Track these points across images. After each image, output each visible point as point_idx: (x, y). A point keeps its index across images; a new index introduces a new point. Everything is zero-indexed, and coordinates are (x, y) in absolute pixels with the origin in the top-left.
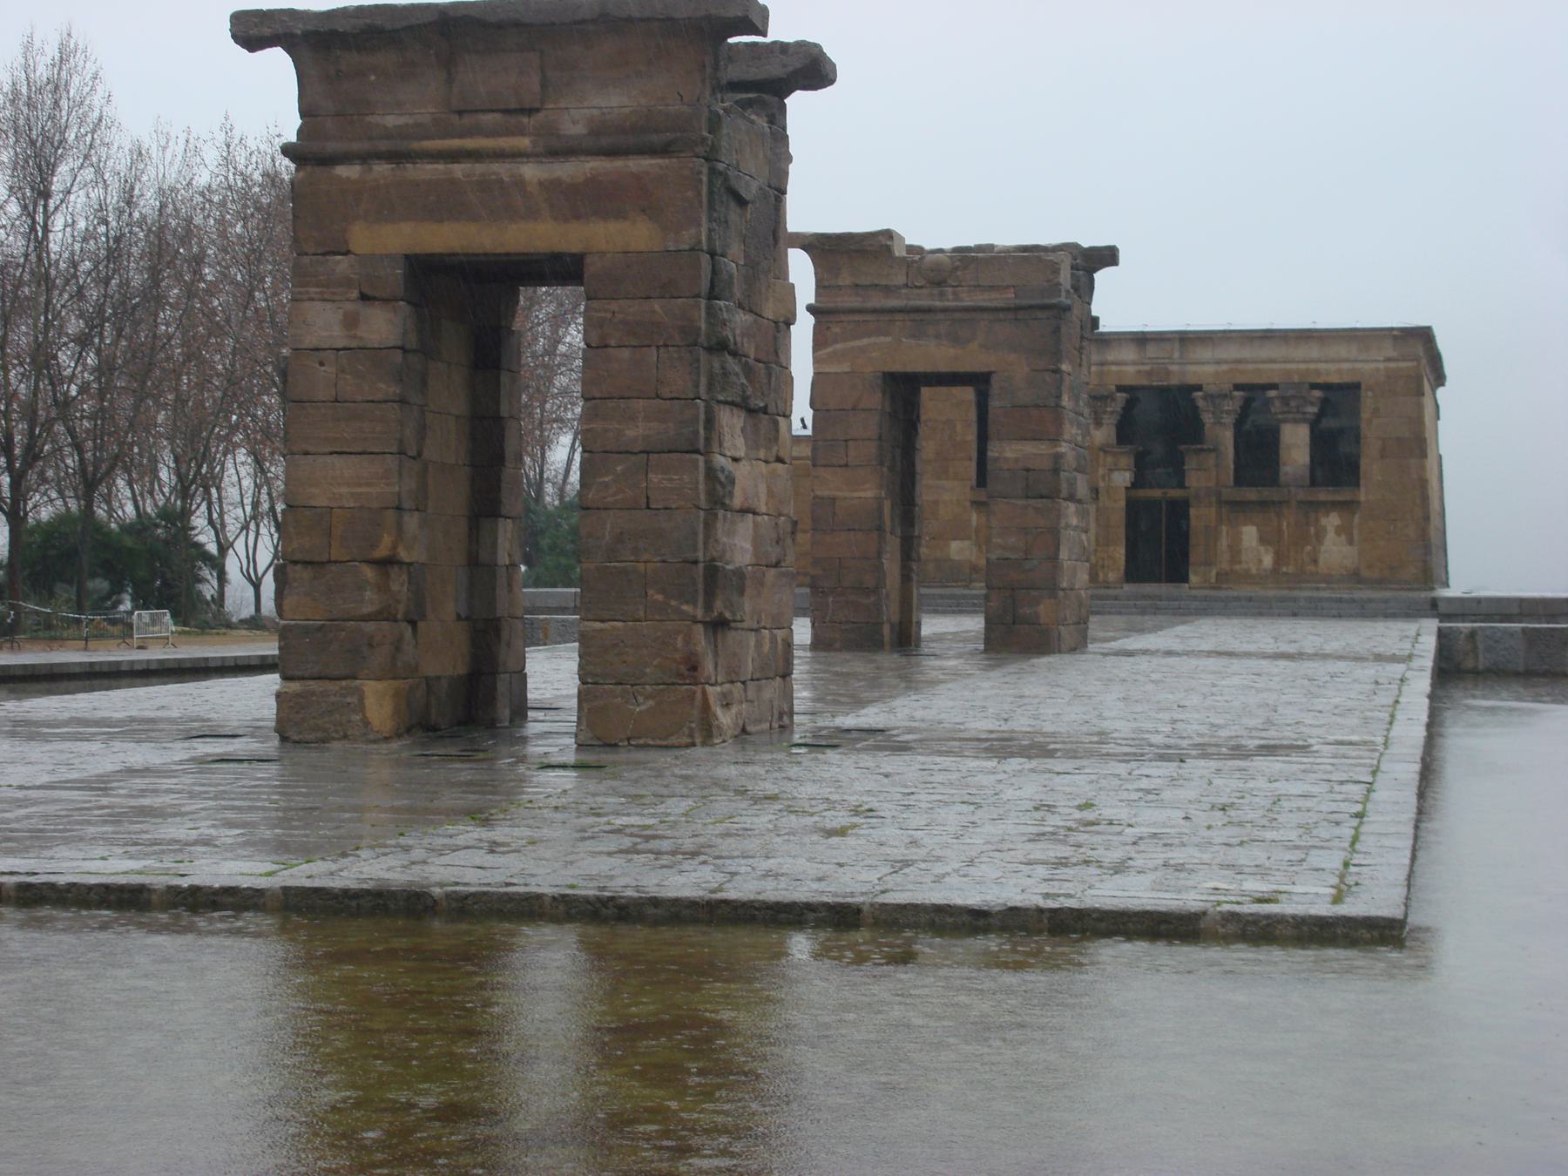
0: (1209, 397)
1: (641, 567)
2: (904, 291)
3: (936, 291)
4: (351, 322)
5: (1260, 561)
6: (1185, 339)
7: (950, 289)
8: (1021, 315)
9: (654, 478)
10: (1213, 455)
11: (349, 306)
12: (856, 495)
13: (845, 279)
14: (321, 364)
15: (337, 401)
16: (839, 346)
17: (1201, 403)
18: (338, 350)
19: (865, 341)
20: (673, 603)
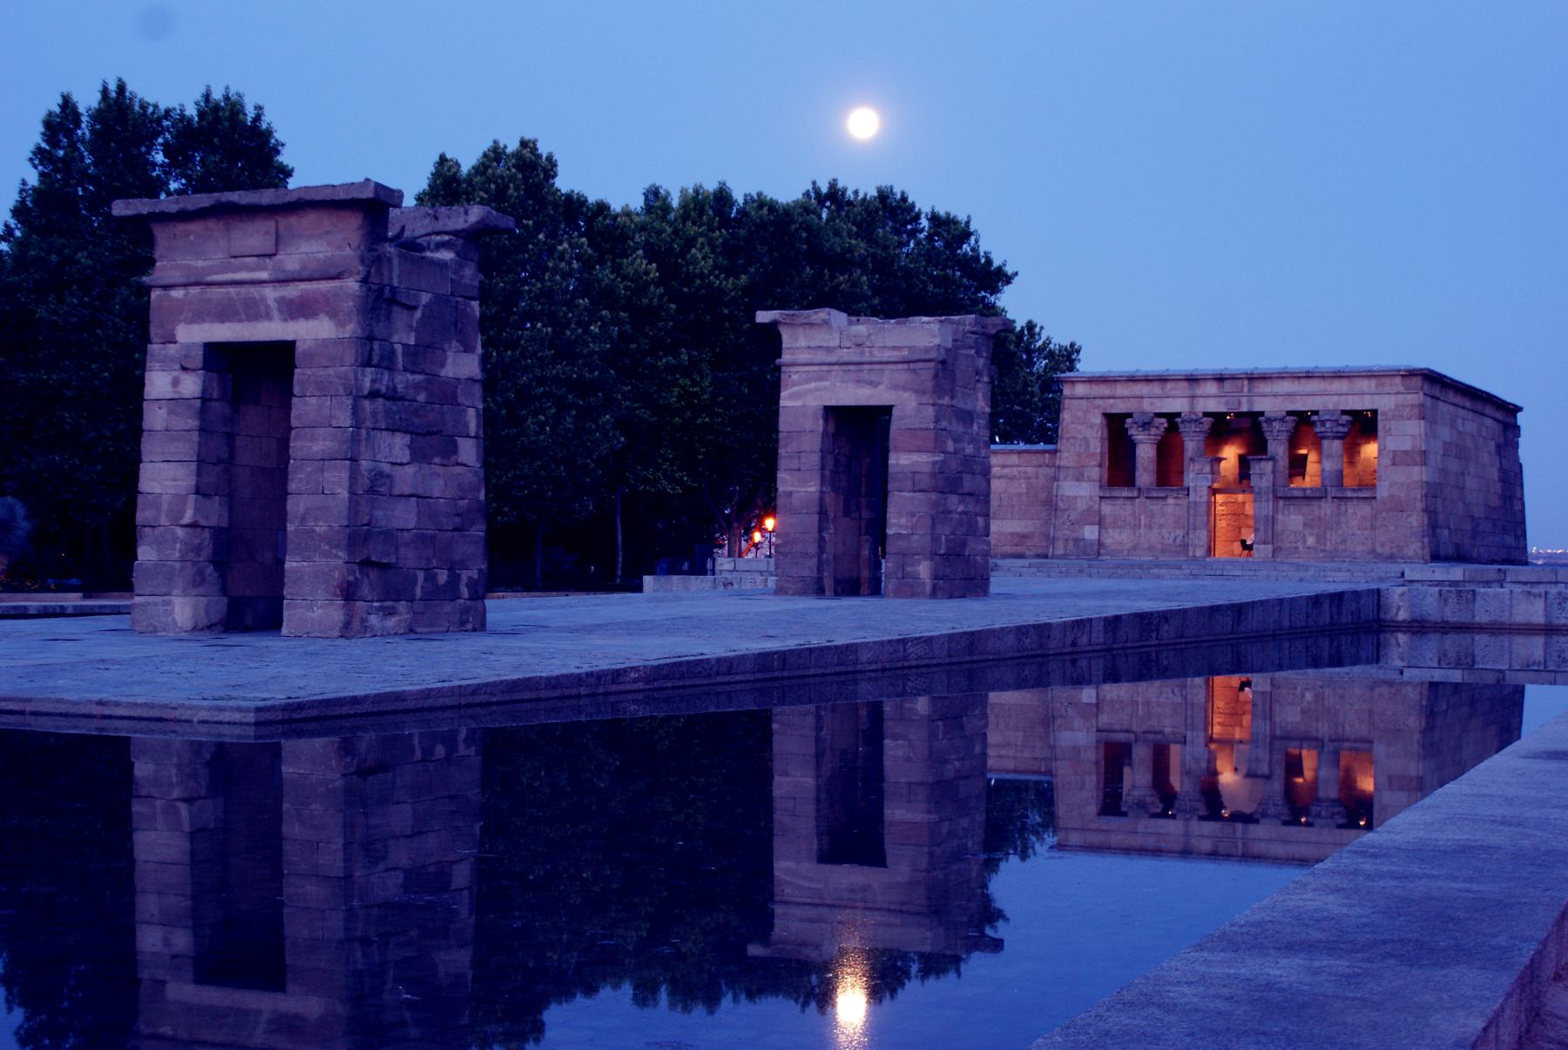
0: (1269, 421)
1: (317, 529)
2: (839, 350)
3: (859, 350)
4: (176, 383)
5: (1305, 542)
6: (1252, 378)
7: (867, 350)
8: (912, 366)
9: (326, 474)
10: (1271, 463)
11: (175, 374)
12: (804, 490)
13: (802, 342)
14: (160, 408)
16: (796, 389)
17: (1264, 425)
19: (813, 385)
20: (334, 551)
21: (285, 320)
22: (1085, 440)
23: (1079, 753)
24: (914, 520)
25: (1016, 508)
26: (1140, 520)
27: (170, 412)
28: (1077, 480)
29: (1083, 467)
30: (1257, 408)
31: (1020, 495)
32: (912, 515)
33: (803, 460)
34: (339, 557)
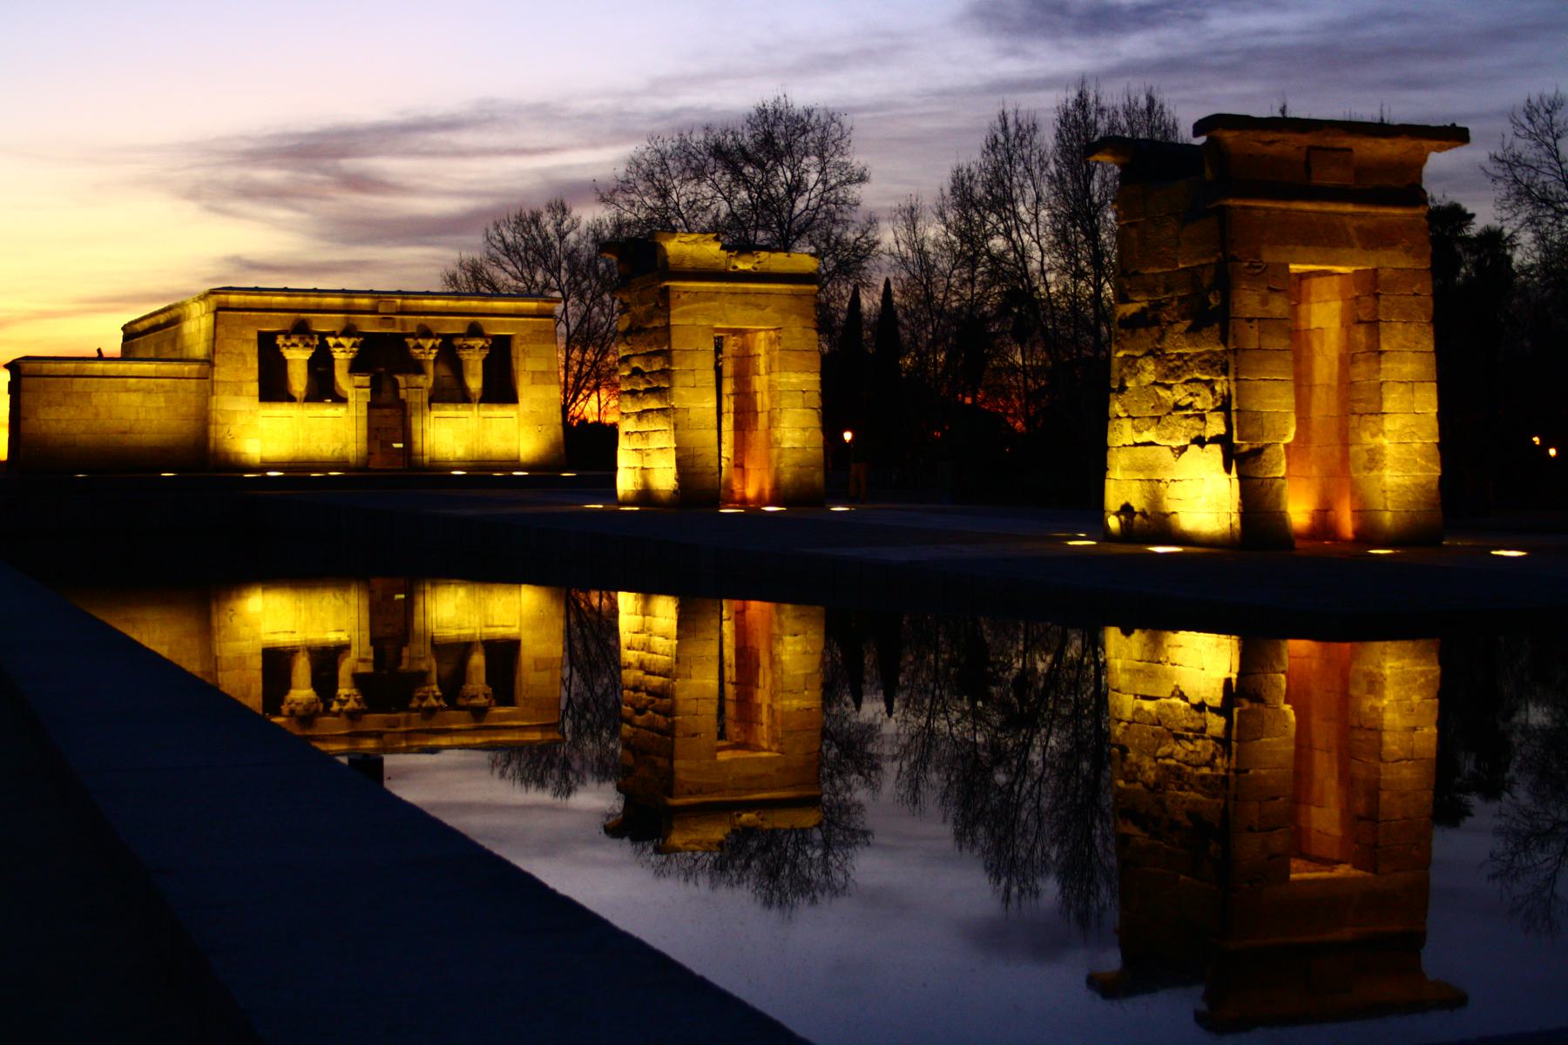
4: (1264, 302)
9: (1418, 395)
14: (1251, 327)
15: (1260, 349)
16: (685, 308)
18: (1260, 319)
19: (701, 305)
20: (1430, 465)
21: (1365, 248)
22: (242, 354)
23: (244, 662)
24: (807, 434)
26: (298, 433)
27: (1261, 332)
28: (236, 394)
29: (240, 381)
30: (409, 331)
31: (158, 409)
32: (804, 429)
33: (698, 377)
34: (1435, 471)
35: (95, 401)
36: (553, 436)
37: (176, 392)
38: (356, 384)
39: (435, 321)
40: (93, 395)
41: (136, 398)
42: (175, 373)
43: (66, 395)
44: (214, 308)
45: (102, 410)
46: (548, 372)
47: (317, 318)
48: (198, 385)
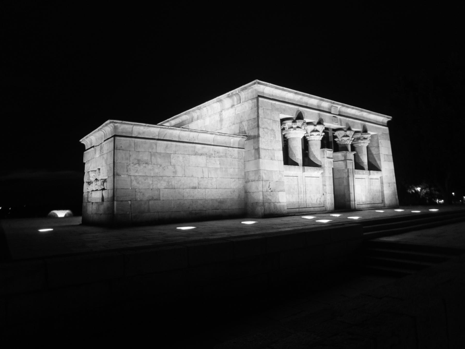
22: (272, 130)
25: (214, 180)
28: (272, 159)
29: (273, 150)
31: (216, 169)
35: (173, 161)
36: (393, 189)
37: (226, 157)
38: (328, 156)
39: (353, 122)
40: (172, 156)
41: (201, 160)
42: (225, 143)
43: (152, 155)
44: (257, 96)
45: (179, 169)
46: (388, 155)
47: (307, 112)
48: (239, 153)
